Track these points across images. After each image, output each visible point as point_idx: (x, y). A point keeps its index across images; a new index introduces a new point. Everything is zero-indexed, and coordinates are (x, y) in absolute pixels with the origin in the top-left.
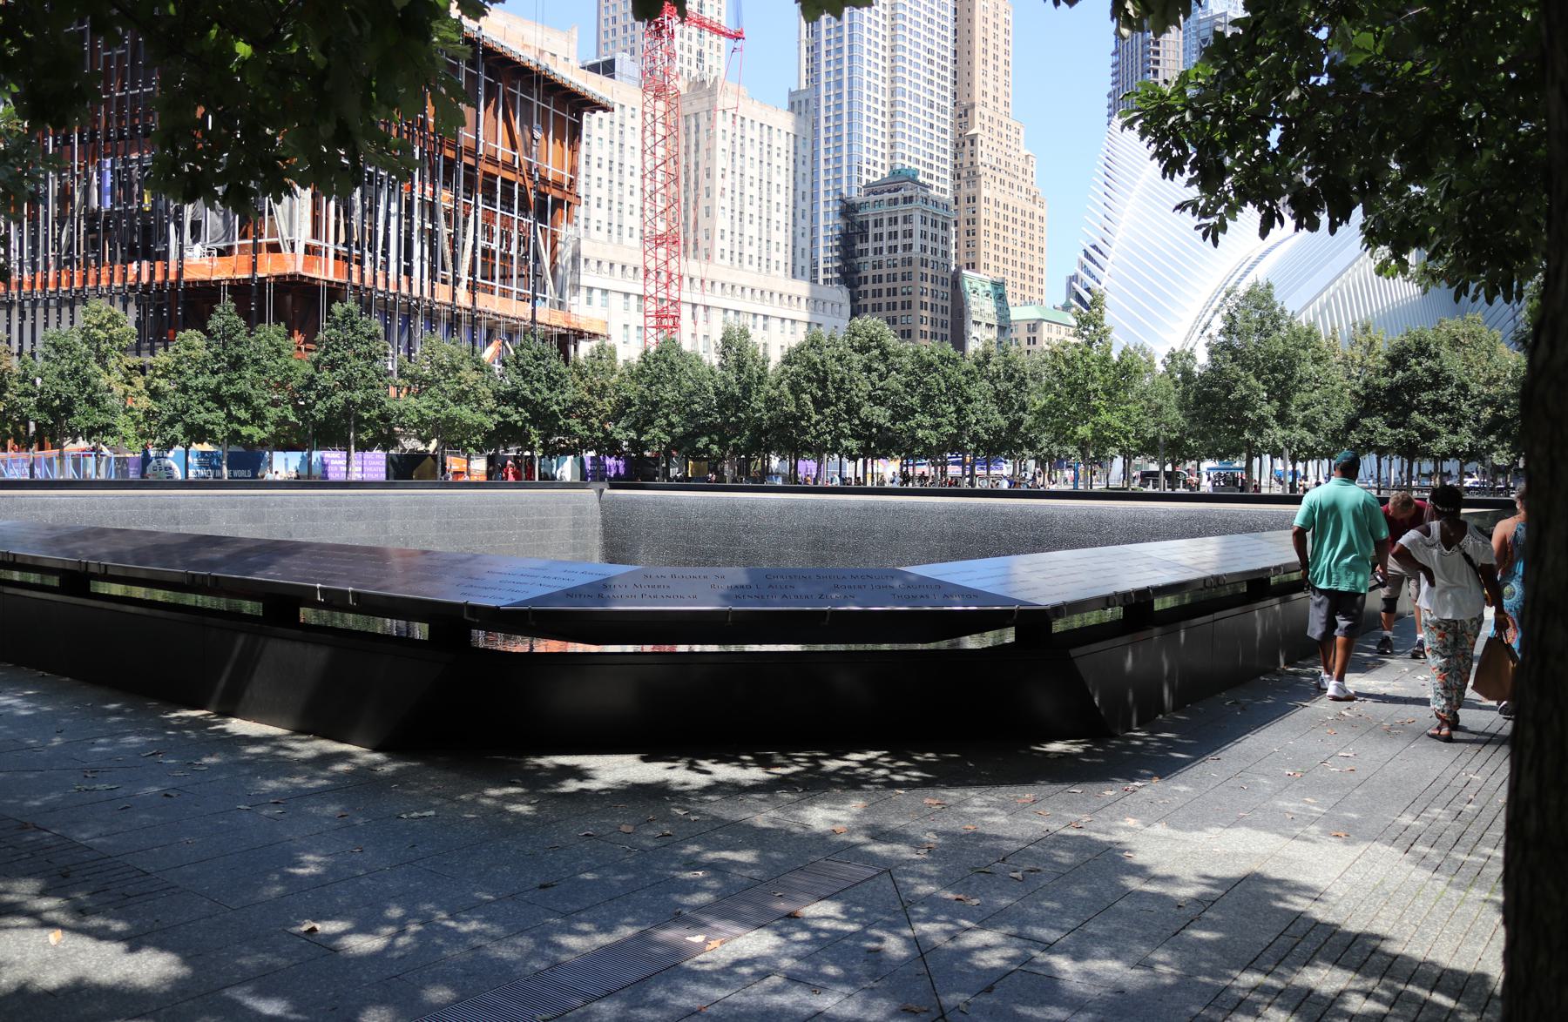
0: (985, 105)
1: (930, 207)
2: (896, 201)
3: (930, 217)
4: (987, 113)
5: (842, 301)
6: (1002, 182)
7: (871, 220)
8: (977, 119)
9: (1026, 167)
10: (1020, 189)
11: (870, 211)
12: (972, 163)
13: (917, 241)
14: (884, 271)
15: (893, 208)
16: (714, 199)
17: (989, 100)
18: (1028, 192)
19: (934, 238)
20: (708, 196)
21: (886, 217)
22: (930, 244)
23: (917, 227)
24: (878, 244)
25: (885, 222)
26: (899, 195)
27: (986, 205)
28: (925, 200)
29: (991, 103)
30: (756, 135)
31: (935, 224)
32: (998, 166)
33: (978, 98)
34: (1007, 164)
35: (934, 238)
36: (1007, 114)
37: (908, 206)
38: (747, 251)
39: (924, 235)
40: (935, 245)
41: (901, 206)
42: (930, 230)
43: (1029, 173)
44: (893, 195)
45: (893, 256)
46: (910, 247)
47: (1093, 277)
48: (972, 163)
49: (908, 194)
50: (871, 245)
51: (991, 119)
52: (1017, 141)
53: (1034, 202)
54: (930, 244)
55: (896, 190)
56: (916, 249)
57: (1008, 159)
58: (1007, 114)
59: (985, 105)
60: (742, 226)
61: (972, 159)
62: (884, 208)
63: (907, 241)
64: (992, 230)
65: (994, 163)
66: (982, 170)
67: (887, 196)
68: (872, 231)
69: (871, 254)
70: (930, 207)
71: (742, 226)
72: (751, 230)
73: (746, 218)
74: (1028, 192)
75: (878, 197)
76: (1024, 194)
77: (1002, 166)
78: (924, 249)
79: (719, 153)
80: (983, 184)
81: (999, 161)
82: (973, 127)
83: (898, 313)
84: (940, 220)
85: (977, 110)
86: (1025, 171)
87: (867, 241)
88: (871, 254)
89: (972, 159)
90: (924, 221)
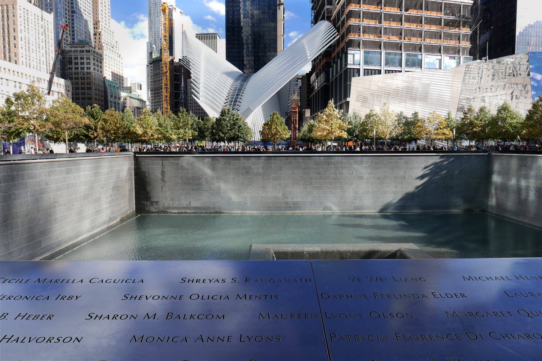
0: (102, 22)
1: (95, 55)
2: (83, 51)
3: (96, 58)
4: (104, 25)
5: (69, 85)
6: (110, 50)
7: (73, 57)
8: (101, 27)
9: (116, 45)
10: (115, 52)
11: (72, 54)
12: (100, 42)
13: (92, 67)
14: (80, 76)
15: (82, 54)
16: (18, 41)
17: (104, 21)
18: (118, 54)
19: (98, 66)
20: (15, 39)
21: (79, 57)
22: (97, 68)
23: (92, 61)
24: (77, 66)
25: (79, 58)
26: (85, 49)
27: (105, 57)
28: (94, 52)
29: (104, 22)
30: (33, 18)
31: (97, 61)
32: (108, 44)
33: (100, 19)
34: (111, 44)
35: (98, 66)
36: (109, 26)
37: (88, 54)
38: (32, 63)
39: (94, 64)
40: (98, 68)
41: (85, 53)
42: (96, 63)
43: (117, 48)
44: (82, 49)
45: (83, 71)
46: (90, 68)
47: (195, 85)
48: (100, 42)
49: (88, 49)
50: (73, 66)
51: (105, 27)
52: (113, 36)
53: (120, 57)
54: (97, 68)
55: (83, 47)
56: (92, 69)
57: (111, 42)
58: (109, 26)
59: (102, 22)
60: (29, 53)
61: (100, 40)
62: (79, 53)
63: (88, 66)
64: (107, 65)
65: (107, 43)
66: (104, 45)
67: (79, 49)
68: (73, 61)
69: (73, 69)
70: (95, 55)
71: (29, 53)
72: (33, 55)
73: (31, 51)
74: (118, 54)
75: (76, 49)
76: (116, 54)
77: (109, 44)
78: (94, 69)
79: (19, 23)
80: (104, 49)
81: (108, 42)
82: (99, 29)
83: (86, 91)
84: (99, 60)
85: (101, 23)
86: (116, 47)
87: (72, 64)
88: (73, 69)
89: (100, 40)
90: (94, 59)
